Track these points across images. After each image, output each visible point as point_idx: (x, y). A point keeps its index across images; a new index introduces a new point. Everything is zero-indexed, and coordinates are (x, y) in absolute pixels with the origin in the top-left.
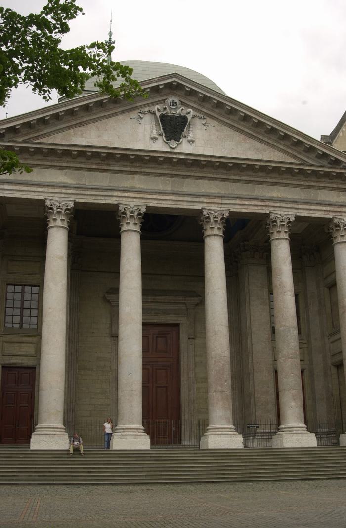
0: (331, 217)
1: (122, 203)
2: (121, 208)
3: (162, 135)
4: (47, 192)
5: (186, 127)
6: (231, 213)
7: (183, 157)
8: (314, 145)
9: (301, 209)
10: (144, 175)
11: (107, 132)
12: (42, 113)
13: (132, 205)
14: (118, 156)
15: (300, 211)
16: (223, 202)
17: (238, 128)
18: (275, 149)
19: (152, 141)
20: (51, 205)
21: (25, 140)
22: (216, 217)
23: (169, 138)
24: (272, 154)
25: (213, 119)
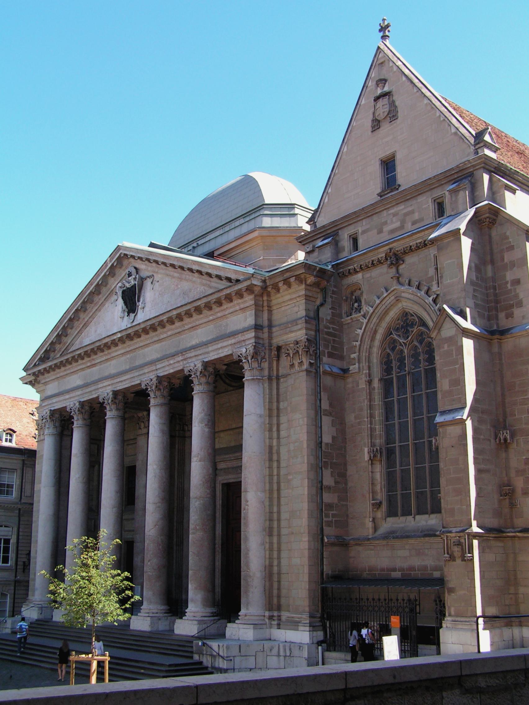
2: (101, 400)
12: (56, 331)
21: (61, 355)
24: (195, 292)
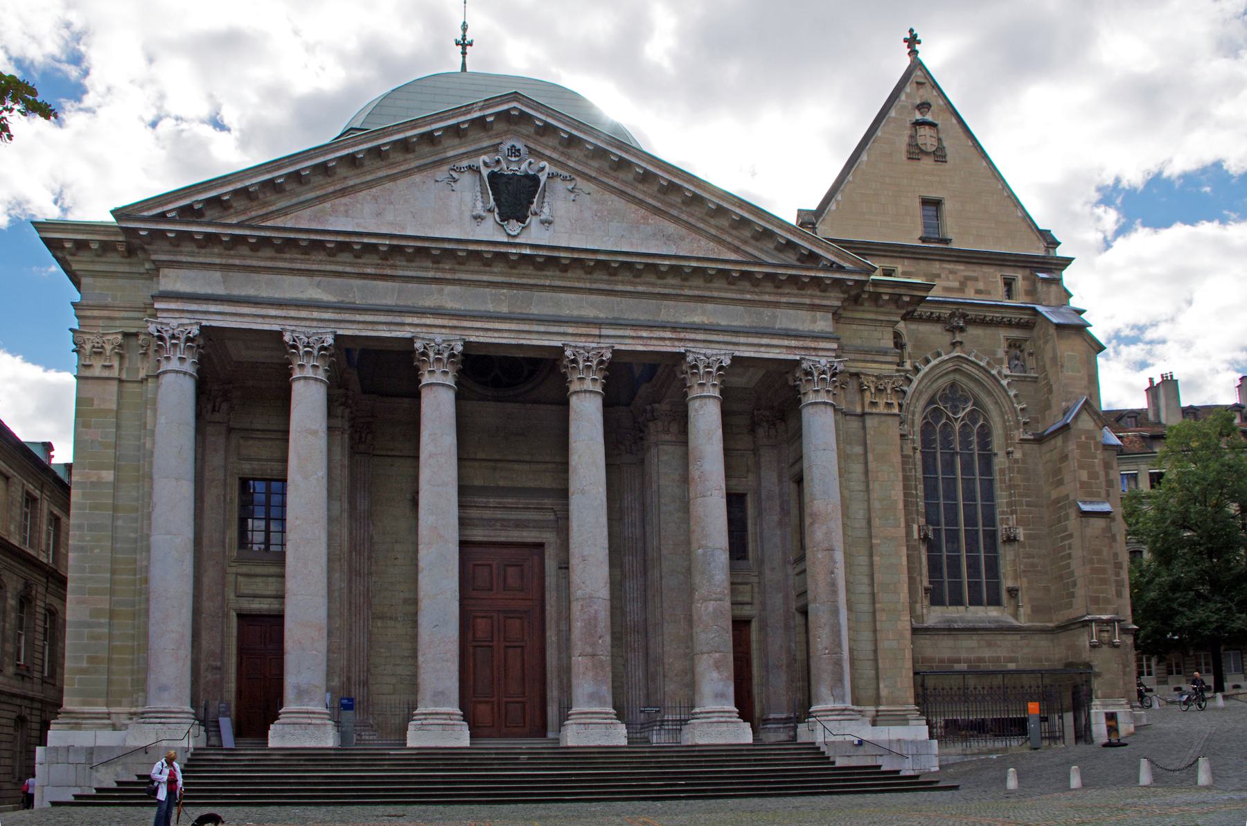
0: (798, 358)
1: (421, 335)
2: (418, 345)
3: (493, 211)
4: (285, 318)
5: (537, 196)
6: (616, 353)
7: (528, 251)
8: (770, 227)
9: (743, 344)
10: (460, 284)
11: (392, 207)
13: (439, 339)
14: (410, 250)
15: (742, 348)
16: (602, 334)
17: (634, 197)
18: (700, 235)
19: (474, 223)
20: (294, 341)
22: (588, 360)
23: (505, 217)
24: (695, 245)
25: (588, 180)
